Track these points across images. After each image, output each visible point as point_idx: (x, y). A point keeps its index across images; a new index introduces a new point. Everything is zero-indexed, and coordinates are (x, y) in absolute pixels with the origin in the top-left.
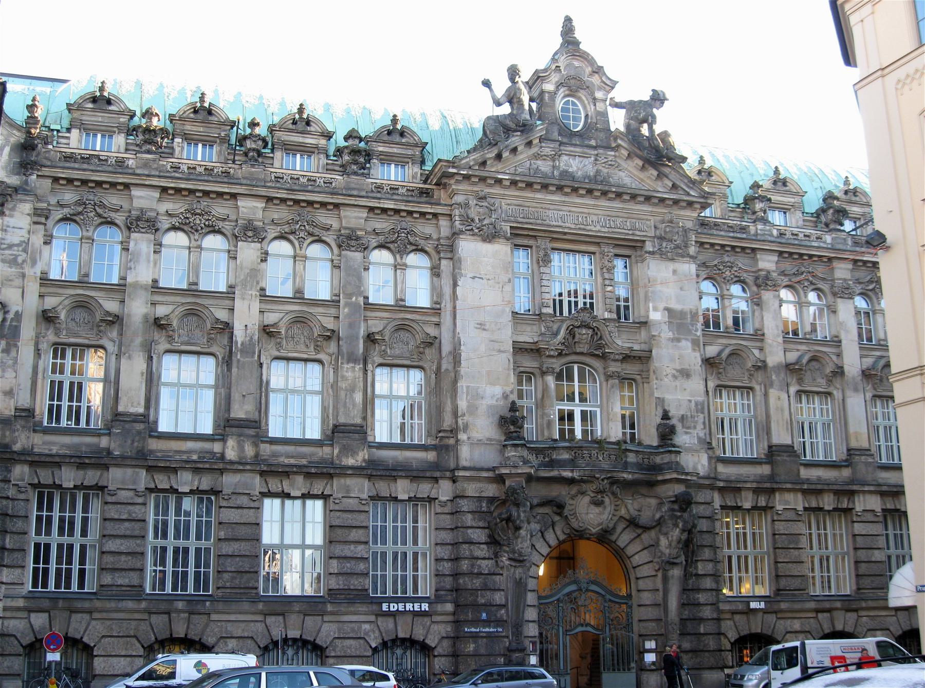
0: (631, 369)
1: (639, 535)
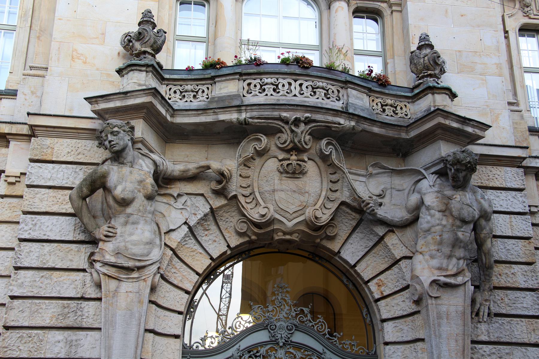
1: (382, 238)
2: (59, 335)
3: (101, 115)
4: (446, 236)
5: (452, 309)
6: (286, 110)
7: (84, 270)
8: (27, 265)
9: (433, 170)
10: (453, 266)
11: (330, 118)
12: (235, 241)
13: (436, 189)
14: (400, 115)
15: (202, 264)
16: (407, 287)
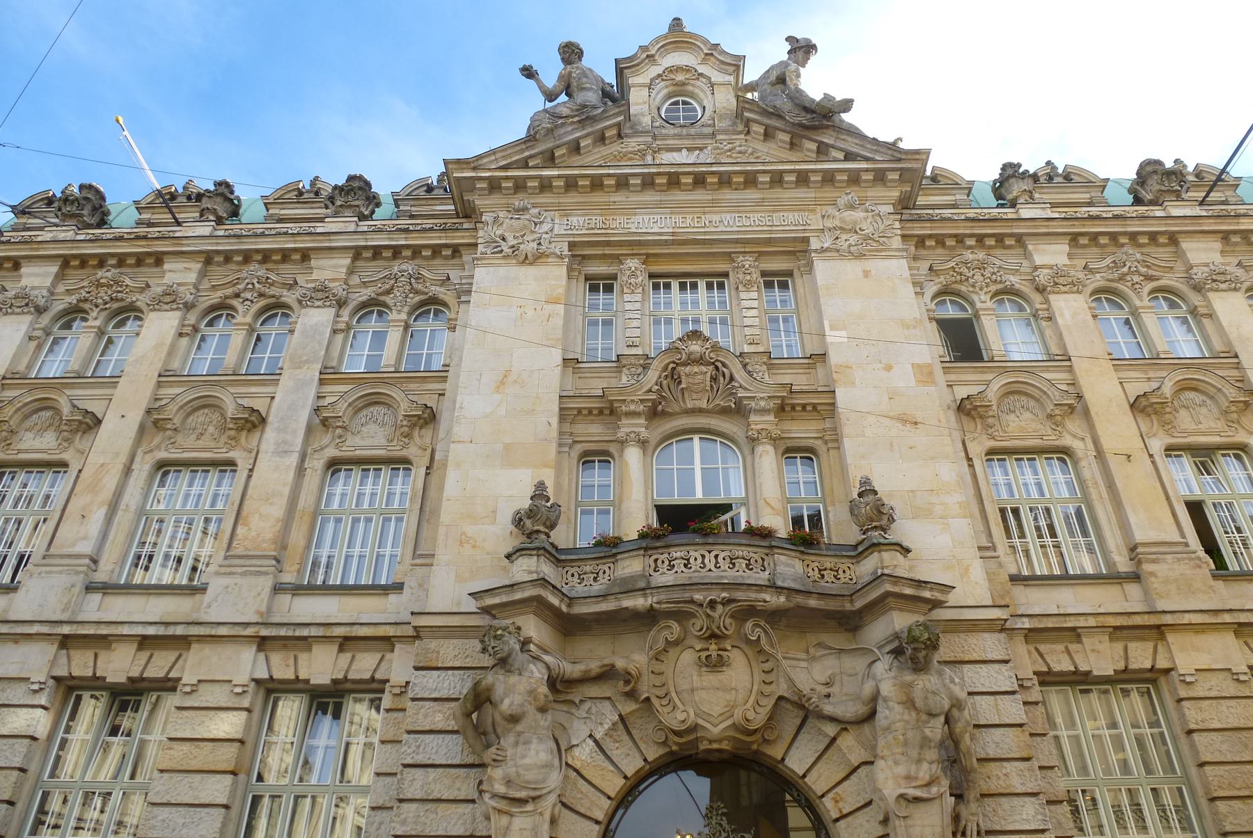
0: (803, 431)
1: (834, 740)
3: (486, 610)
4: (910, 734)
5: (928, 831)
6: (698, 591)
7: (473, 801)
8: (410, 796)
9: (888, 648)
10: (925, 772)
11: (753, 595)
12: (653, 753)
13: (892, 674)
14: (843, 580)
15: (615, 785)
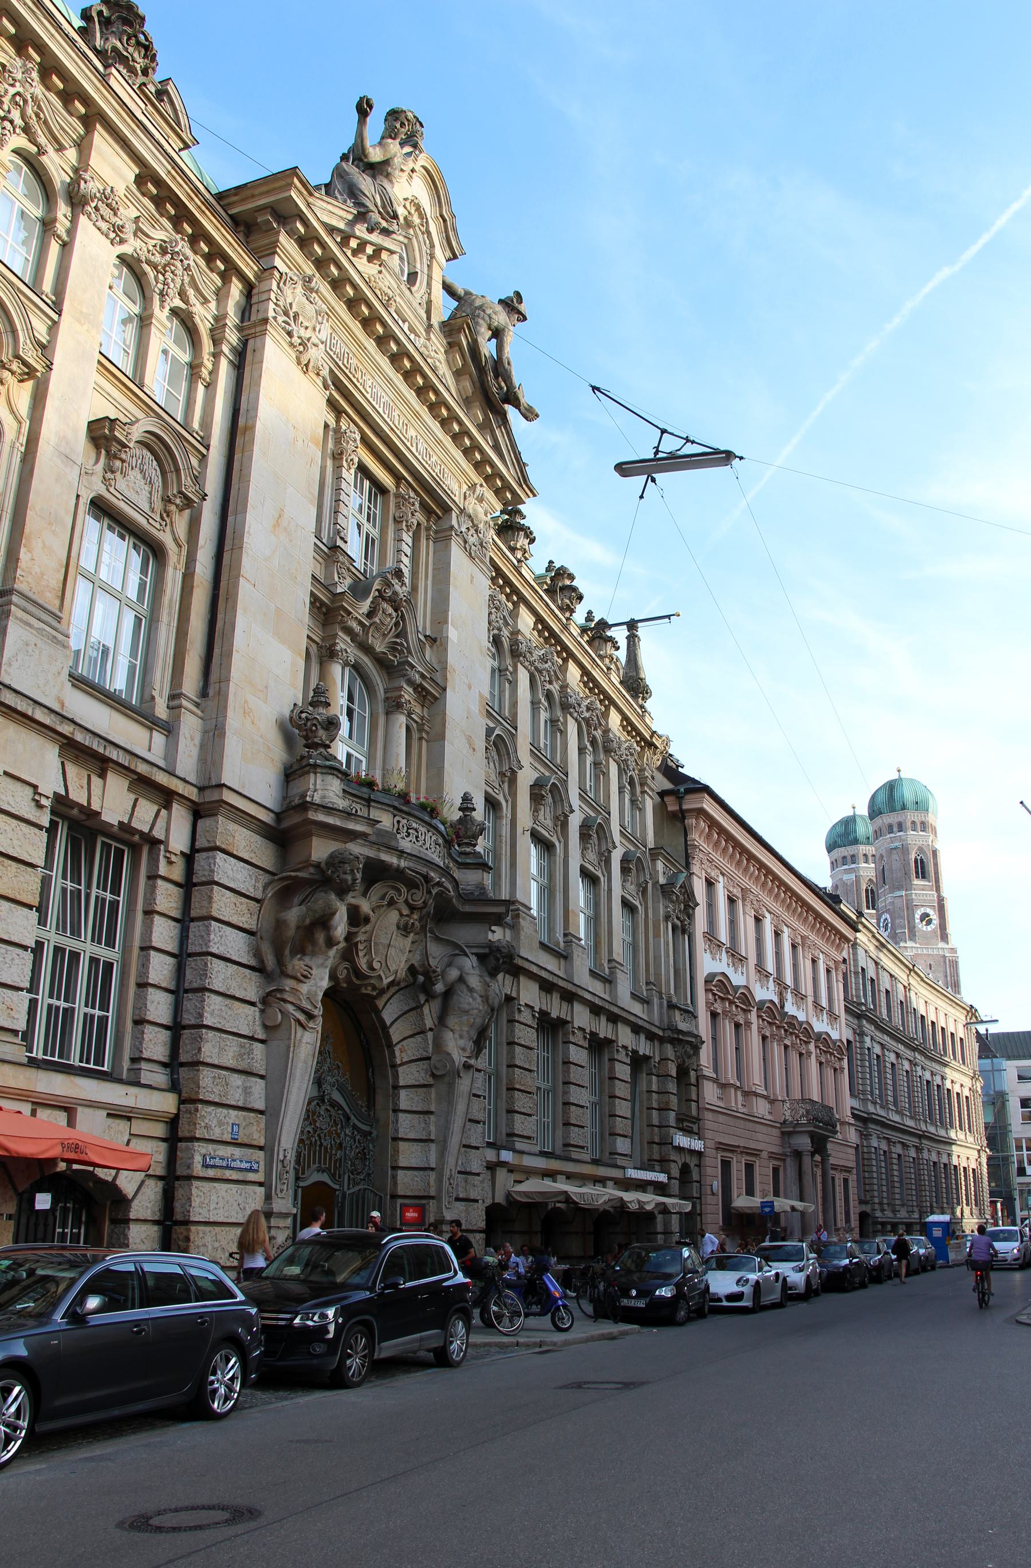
2: (237, 1080)
16: (429, 1058)
